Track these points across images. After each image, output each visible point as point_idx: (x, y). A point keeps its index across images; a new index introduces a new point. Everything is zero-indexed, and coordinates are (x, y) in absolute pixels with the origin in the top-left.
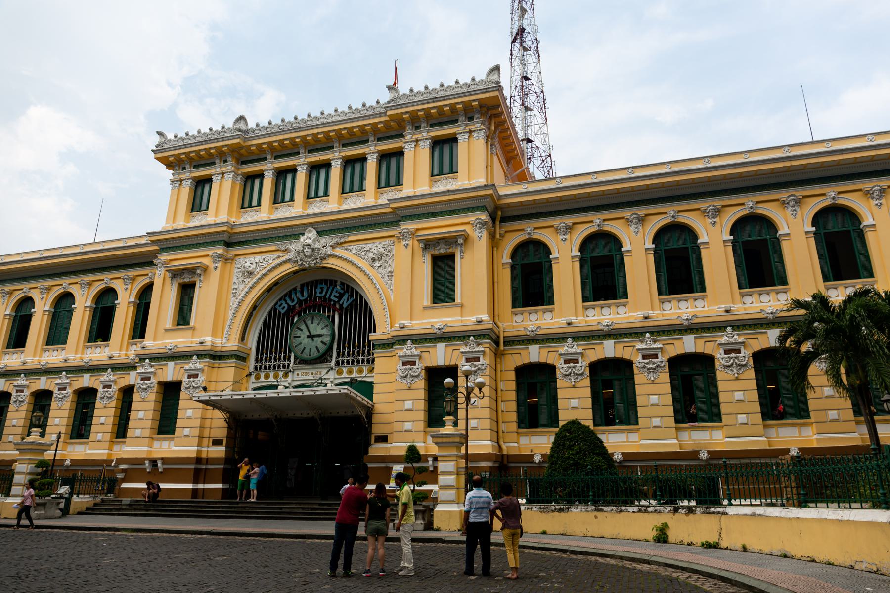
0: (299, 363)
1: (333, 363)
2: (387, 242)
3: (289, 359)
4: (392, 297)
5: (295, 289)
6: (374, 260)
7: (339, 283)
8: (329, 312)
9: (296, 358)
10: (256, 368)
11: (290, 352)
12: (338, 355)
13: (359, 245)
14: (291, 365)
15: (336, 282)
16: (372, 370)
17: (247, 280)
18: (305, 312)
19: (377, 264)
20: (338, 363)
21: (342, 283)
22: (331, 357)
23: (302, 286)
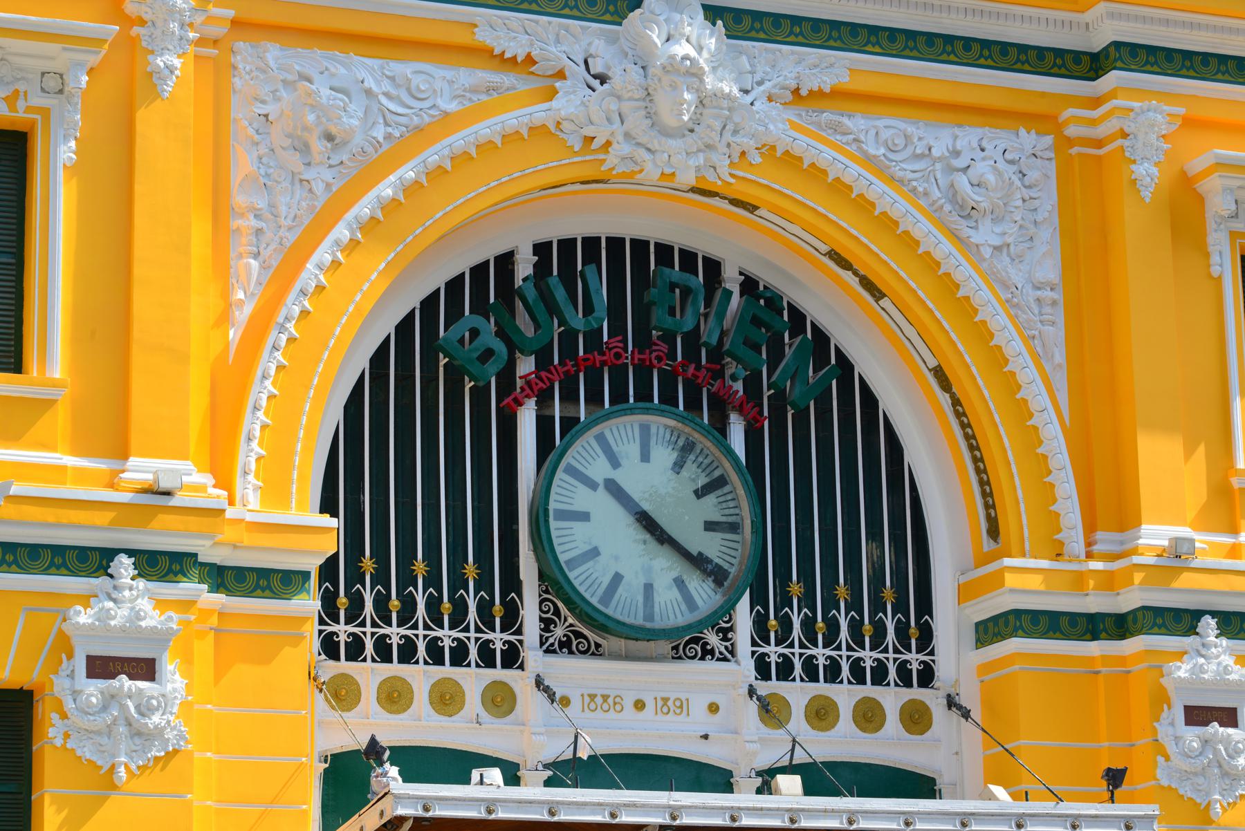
0: (565, 645)
1: (747, 666)
2: (1027, 139)
3: (511, 620)
4: (1063, 398)
5: (506, 261)
6: (969, 212)
7: (731, 279)
8: (693, 404)
9: (547, 625)
10: (330, 647)
11: (512, 582)
12: (761, 631)
13: (890, 126)
14: (532, 656)
15: (713, 267)
16: (916, 719)
17: (328, 175)
18: (570, 396)
19: (985, 235)
20: (763, 670)
21: (749, 285)
22: (725, 633)
23: (541, 249)
